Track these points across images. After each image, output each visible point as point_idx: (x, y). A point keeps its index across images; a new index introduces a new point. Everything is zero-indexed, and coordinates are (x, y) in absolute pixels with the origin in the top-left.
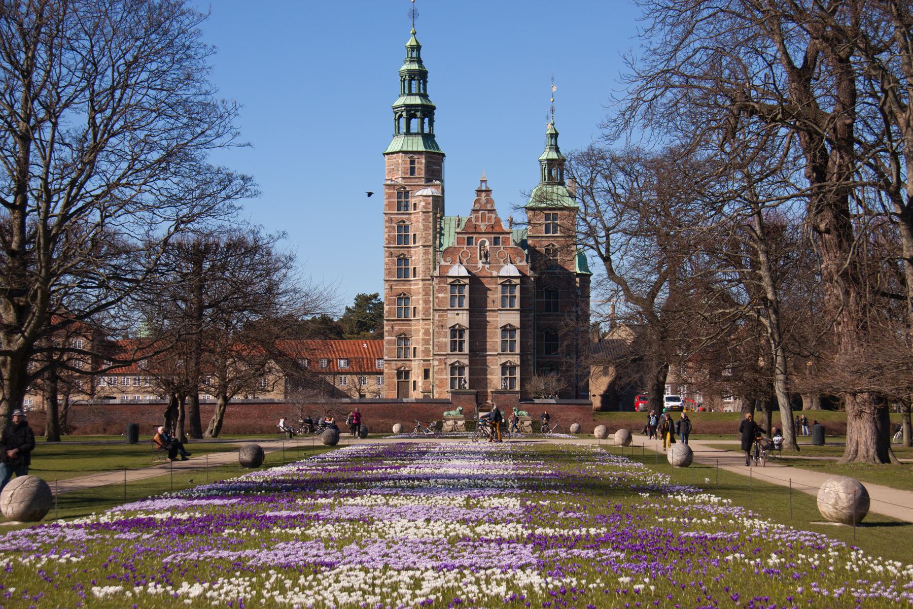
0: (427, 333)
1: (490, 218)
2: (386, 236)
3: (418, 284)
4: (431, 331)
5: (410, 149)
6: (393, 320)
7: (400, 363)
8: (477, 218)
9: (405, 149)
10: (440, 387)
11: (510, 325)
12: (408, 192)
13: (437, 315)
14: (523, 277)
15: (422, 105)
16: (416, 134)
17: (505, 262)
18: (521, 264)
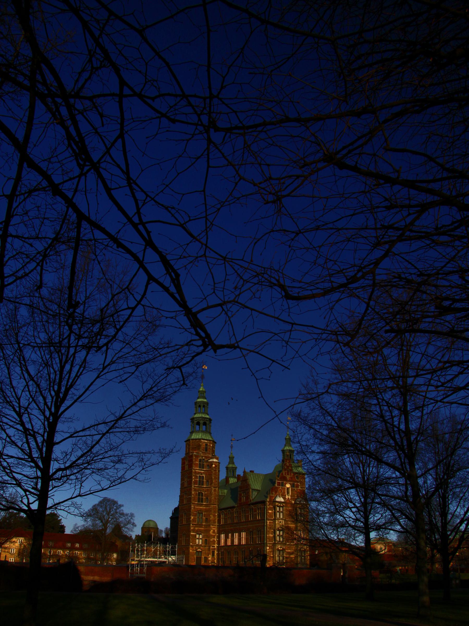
0: (214, 532)
2: (193, 480)
4: (216, 531)
6: (195, 524)
7: (197, 547)
8: (285, 473)
9: (203, 437)
12: (204, 459)
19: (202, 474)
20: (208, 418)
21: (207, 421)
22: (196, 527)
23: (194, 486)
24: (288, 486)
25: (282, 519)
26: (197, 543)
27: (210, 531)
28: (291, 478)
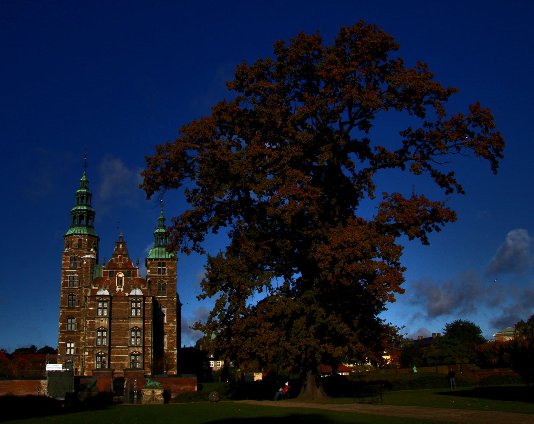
1: (125, 260)
2: (62, 282)
3: (80, 310)
5: (79, 233)
6: (64, 332)
7: (67, 358)
8: (117, 259)
9: (76, 232)
10: (88, 370)
11: (136, 327)
12: (77, 257)
13: (88, 321)
14: (144, 297)
15: (87, 210)
16: (83, 225)
17: (135, 288)
18: (144, 289)
19: (73, 274)
20: (85, 210)
21: (85, 213)
22: (65, 334)
23: (64, 289)
24: (121, 275)
25: (105, 317)
26: (68, 353)
27: (80, 338)
28: (125, 265)
